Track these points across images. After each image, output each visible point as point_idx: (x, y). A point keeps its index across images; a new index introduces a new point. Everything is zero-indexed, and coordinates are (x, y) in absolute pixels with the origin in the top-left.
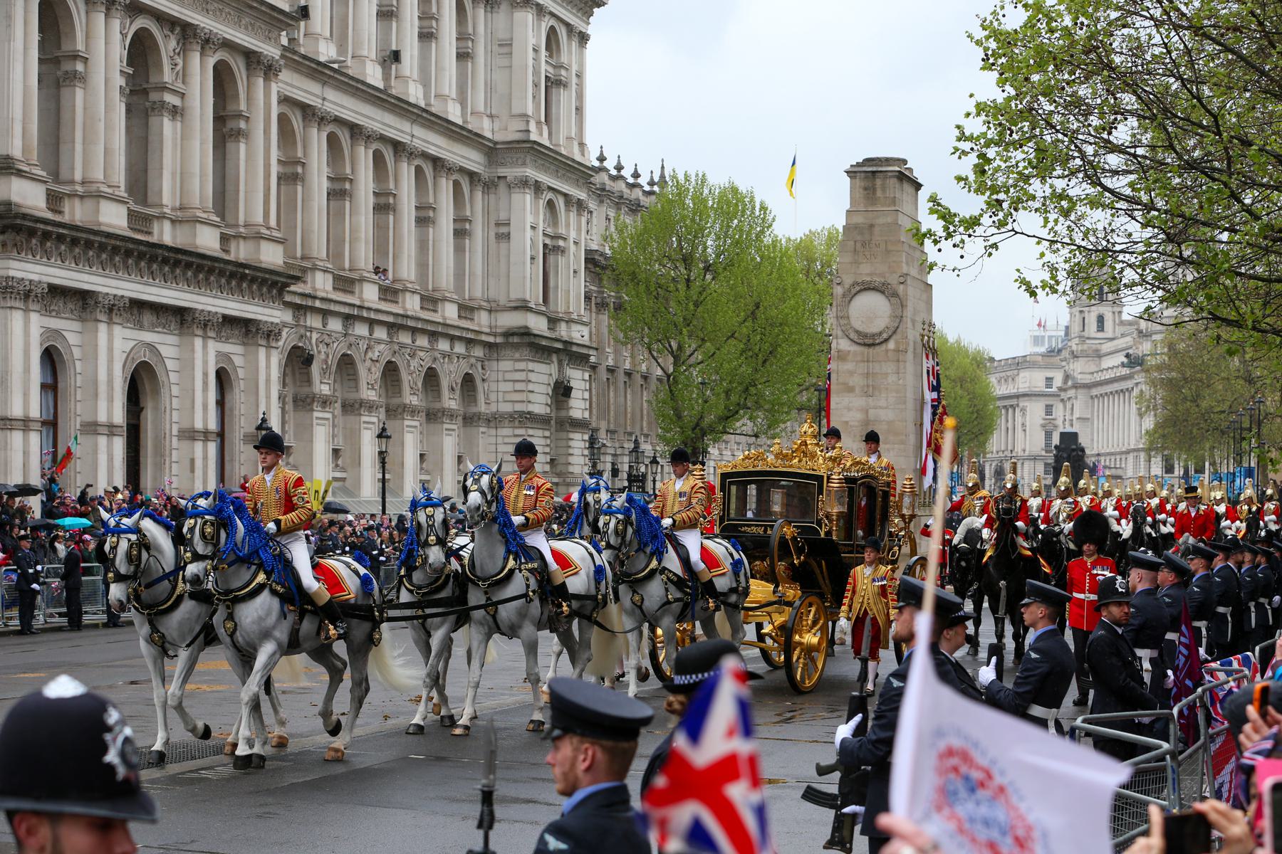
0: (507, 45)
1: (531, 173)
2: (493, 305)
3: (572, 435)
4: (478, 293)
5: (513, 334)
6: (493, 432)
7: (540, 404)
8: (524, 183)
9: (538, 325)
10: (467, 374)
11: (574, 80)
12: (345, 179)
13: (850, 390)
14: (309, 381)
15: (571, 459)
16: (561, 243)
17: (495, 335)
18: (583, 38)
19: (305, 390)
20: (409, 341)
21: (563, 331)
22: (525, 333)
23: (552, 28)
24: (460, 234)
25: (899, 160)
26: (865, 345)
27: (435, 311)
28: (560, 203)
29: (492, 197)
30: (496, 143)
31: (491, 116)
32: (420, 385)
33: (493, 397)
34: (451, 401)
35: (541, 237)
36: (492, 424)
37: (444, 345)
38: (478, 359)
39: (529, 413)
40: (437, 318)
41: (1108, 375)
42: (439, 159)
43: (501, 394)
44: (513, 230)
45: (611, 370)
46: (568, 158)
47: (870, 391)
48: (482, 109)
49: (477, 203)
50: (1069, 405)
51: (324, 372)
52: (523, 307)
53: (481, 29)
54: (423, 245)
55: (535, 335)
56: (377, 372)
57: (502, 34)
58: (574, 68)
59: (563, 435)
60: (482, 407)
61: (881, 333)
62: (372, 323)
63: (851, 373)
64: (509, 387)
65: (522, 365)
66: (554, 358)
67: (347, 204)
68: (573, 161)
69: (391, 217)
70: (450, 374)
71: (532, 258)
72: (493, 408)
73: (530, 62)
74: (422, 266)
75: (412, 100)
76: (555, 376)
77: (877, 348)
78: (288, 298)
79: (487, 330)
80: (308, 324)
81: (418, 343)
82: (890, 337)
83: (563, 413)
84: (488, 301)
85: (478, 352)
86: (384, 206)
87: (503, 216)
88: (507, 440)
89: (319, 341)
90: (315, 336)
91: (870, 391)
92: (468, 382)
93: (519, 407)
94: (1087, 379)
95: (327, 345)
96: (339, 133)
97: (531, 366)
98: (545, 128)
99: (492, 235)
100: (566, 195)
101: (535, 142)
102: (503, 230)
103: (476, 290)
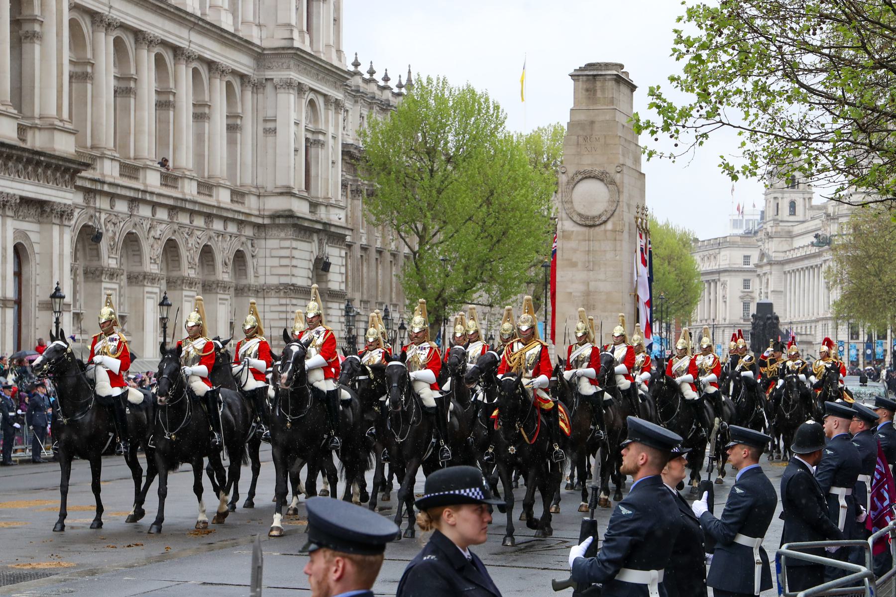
1: (295, 76)
2: (262, 191)
4: (248, 180)
5: (279, 217)
7: (302, 277)
9: (301, 208)
10: (238, 251)
12: (130, 79)
13: (574, 265)
14: (98, 255)
16: (321, 137)
17: (263, 217)
19: (95, 264)
20: (187, 221)
21: (323, 214)
22: (290, 215)
24: (232, 128)
25: (616, 65)
26: (586, 226)
27: (210, 196)
28: (320, 102)
29: (260, 96)
30: (264, 49)
31: (259, 25)
32: (197, 260)
33: (261, 271)
34: (224, 275)
36: (260, 295)
37: (218, 225)
38: (248, 238)
39: (293, 285)
41: (799, 254)
42: (213, 62)
43: (268, 269)
44: (279, 125)
45: (364, 249)
46: (327, 63)
47: (590, 266)
48: (251, 19)
49: (247, 100)
50: (764, 280)
51: (112, 248)
52: (288, 193)
54: (199, 138)
55: (299, 218)
56: (159, 249)
60: (251, 280)
61: (600, 216)
62: (155, 205)
63: (575, 250)
64: (276, 262)
65: (287, 244)
67: (132, 100)
68: (332, 65)
69: (171, 113)
70: (223, 251)
71: (296, 150)
72: (261, 281)
74: (199, 156)
75: (189, 10)
76: (316, 253)
77: (597, 228)
78: (79, 183)
79: (257, 213)
80: (98, 205)
81: (196, 223)
82: (608, 219)
83: (323, 286)
84: (257, 187)
85: (249, 232)
86: (165, 103)
87: (270, 114)
88: (273, 309)
89: (107, 221)
90: (103, 216)
91: (590, 266)
92: (239, 257)
93: (284, 280)
94: (781, 257)
95: (115, 224)
96: (124, 37)
97: (295, 244)
98: (307, 37)
100: (325, 96)
101: (298, 49)
102: (270, 125)
103: (246, 178)
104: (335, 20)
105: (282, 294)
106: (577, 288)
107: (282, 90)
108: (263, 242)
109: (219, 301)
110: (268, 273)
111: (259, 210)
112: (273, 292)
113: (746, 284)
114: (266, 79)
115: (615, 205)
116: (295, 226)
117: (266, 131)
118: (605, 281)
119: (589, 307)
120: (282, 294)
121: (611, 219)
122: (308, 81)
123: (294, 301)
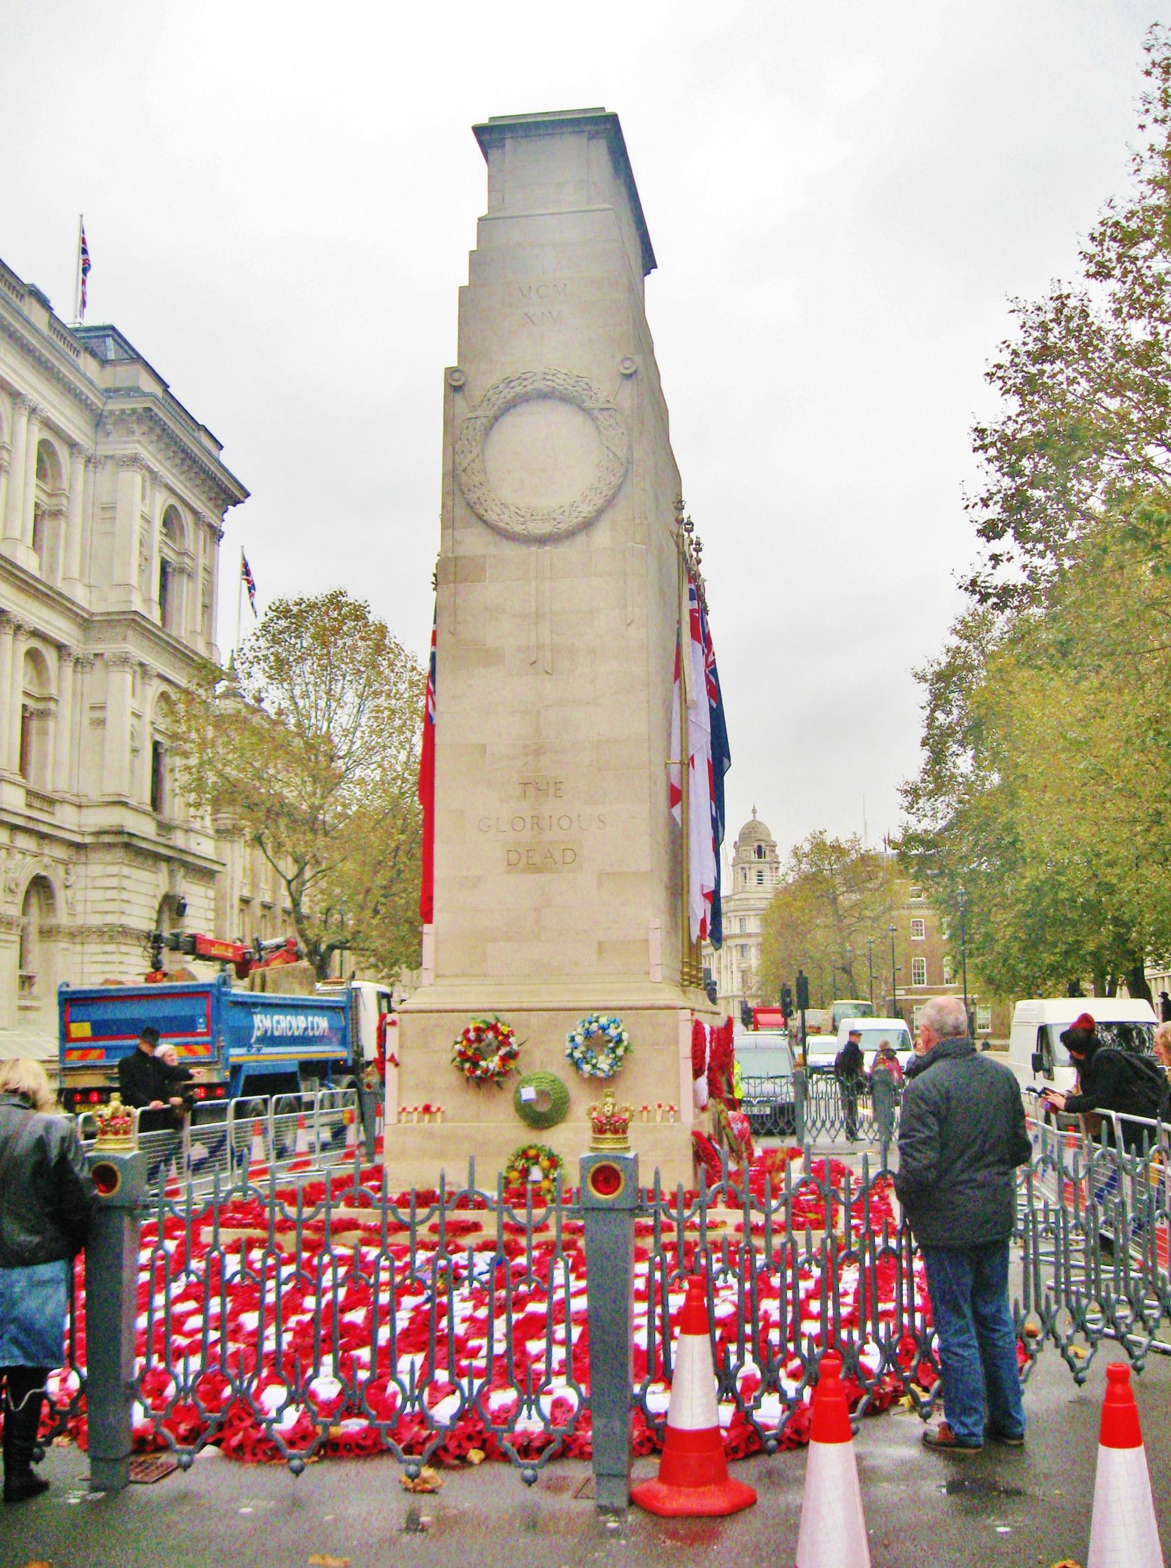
0: (109, 508)
2: (84, 800)
4: (63, 785)
6: (78, 948)
7: (142, 918)
8: (124, 661)
9: (144, 827)
17: (83, 834)
18: (216, 534)
21: (179, 839)
23: (172, 508)
30: (93, 614)
33: (80, 907)
35: (149, 729)
36: (78, 940)
44: (110, 714)
45: (266, 907)
46: (186, 647)
47: (540, 662)
48: (76, 574)
49: (63, 680)
53: (79, 487)
58: (202, 561)
60: (62, 918)
66: (164, 866)
71: (135, 751)
72: (79, 921)
82: (600, 512)
85: (61, 852)
87: (98, 699)
93: (110, 919)
97: (126, 870)
99: (86, 722)
102: (98, 714)
104: (205, 606)
105: (106, 938)
116: (127, 846)
120: (106, 938)
122: (157, 664)
123: (124, 949)
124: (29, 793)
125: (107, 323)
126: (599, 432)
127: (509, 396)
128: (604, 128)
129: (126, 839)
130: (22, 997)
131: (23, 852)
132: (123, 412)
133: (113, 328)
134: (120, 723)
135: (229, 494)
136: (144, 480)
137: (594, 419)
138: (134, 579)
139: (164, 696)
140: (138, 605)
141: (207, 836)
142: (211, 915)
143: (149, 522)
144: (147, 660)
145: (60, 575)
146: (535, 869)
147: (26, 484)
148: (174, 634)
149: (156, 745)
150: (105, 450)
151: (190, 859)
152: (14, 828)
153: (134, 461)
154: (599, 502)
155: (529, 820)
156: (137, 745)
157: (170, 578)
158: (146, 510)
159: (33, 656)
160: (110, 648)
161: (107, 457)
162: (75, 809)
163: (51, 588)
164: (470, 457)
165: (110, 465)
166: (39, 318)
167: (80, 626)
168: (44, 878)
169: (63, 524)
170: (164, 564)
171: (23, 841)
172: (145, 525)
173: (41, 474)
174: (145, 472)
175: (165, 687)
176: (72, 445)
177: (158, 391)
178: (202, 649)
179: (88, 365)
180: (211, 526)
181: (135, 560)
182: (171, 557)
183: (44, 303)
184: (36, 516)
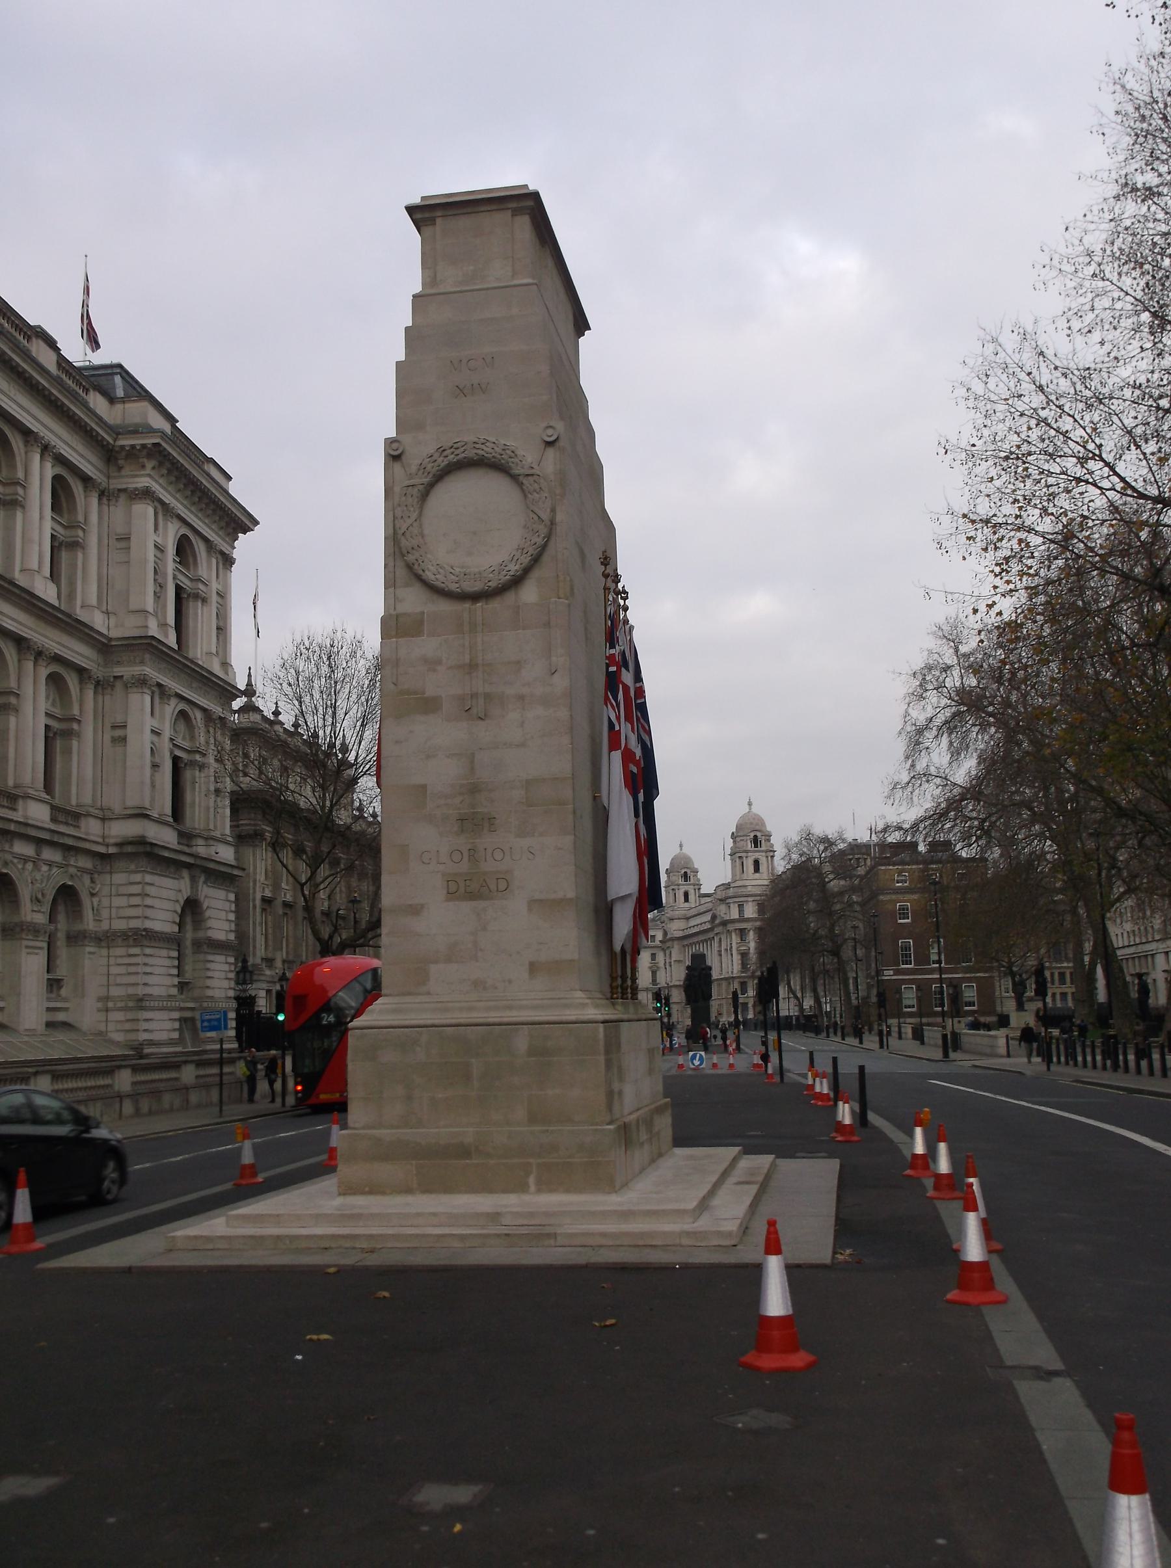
2: (108, 814)
3: (210, 957)
4: (87, 799)
5: (130, 843)
6: (104, 952)
7: (163, 920)
8: (142, 682)
9: (166, 837)
11: (214, 598)
15: (209, 982)
16: (198, 757)
17: (107, 846)
22: (141, 841)
23: (184, 536)
29: (107, 697)
30: (110, 639)
33: (105, 913)
35: (167, 745)
36: (103, 944)
38: (83, 870)
39: (145, 930)
40: (18, 816)
43: (114, 911)
44: (130, 733)
45: (286, 905)
46: (202, 668)
47: (475, 708)
48: (94, 601)
49: (85, 702)
52: (142, 815)
53: (94, 518)
55: (152, 844)
57: (120, 529)
58: (215, 586)
59: (201, 957)
60: (89, 923)
63: (432, 664)
65: (137, 877)
66: (185, 873)
71: (155, 766)
72: (105, 926)
73: (151, 558)
76: (186, 893)
77: (495, 604)
82: (527, 571)
83: (201, 934)
84: (102, 809)
85: (85, 863)
87: (119, 719)
88: (120, 961)
91: (475, 708)
93: (134, 924)
94: (680, 934)
97: (149, 878)
99: (107, 737)
102: (119, 733)
106: (442, 774)
107: (135, 690)
108: (108, 876)
109: (24, 951)
110: (113, 916)
111: (104, 837)
112: (119, 941)
113: (653, 956)
114: (115, 677)
115: (543, 531)
117: (114, 740)
118: (523, 745)
119: (473, 822)
120: (131, 942)
121: (535, 574)
123: (148, 951)
124: (54, 808)
125: (115, 361)
126: (525, 496)
127: (443, 465)
128: (526, 206)
129: (148, 849)
130: (49, 1000)
131: (50, 864)
132: (133, 447)
133: (120, 366)
134: (140, 740)
135: (237, 522)
136: (156, 514)
137: (521, 485)
138: (150, 605)
139: (183, 714)
140: (153, 630)
141: (227, 843)
142: (232, 917)
143: (162, 551)
144: (165, 680)
145: (79, 603)
146: (472, 896)
147: (41, 518)
148: (191, 656)
149: (176, 760)
150: (116, 484)
151: (212, 865)
152: (39, 842)
153: (146, 494)
154: (526, 560)
155: (466, 854)
156: (157, 760)
157: (184, 602)
158: (159, 540)
159: (55, 680)
160: (127, 671)
161: (120, 490)
162: (99, 822)
163: (69, 616)
164: (409, 522)
165: (123, 498)
166: (47, 359)
167: (100, 651)
168: (71, 887)
169: (80, 555)
170: (179, 590)
171: (48, 854)
172: (159, 555)
173: (56, 507)
174: (156, 504)
175: (182, 706)
176: (86, 480)
177: (167, 428)
178: (217, 669)
179: (97, 402)
180: (222, 553)
181: (150, 588)
182: (186, 583)
183: (52, 343)
184: (52, 548)
